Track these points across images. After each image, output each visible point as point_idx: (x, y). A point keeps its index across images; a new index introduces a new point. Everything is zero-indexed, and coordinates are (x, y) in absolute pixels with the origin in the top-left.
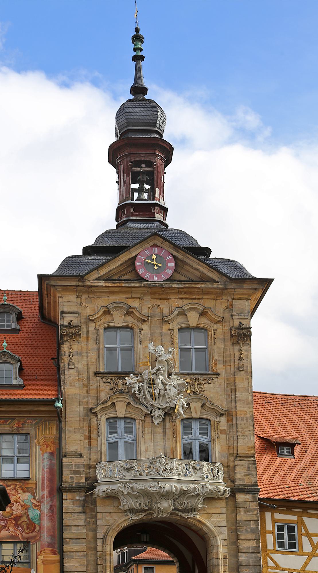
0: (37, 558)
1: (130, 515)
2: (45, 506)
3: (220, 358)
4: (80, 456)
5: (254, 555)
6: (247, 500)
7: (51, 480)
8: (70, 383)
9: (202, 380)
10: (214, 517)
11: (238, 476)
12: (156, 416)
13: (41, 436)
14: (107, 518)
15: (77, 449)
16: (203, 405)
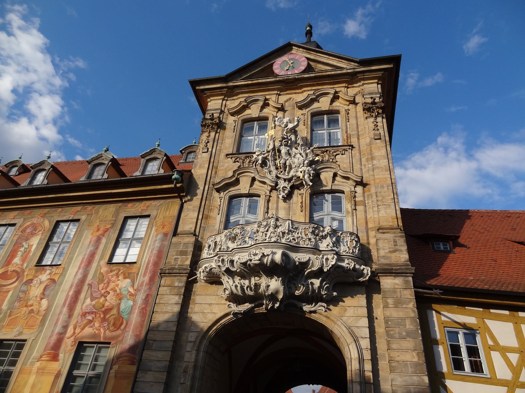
0: (111, 369)
1: (234, 308)
2: (141, 296)
3: (353, 133)
4: (195, 235)
5: (415, 378)
6: (397, 287)
7: (156, 264)
8: (201, 165)
9: (335, 152)
10: (350, 312)
11: (382, 253)
12: (281, 189)
13: (161, 216)
14: (205, 311)
15: (191, 228)
16: (335, 175)
